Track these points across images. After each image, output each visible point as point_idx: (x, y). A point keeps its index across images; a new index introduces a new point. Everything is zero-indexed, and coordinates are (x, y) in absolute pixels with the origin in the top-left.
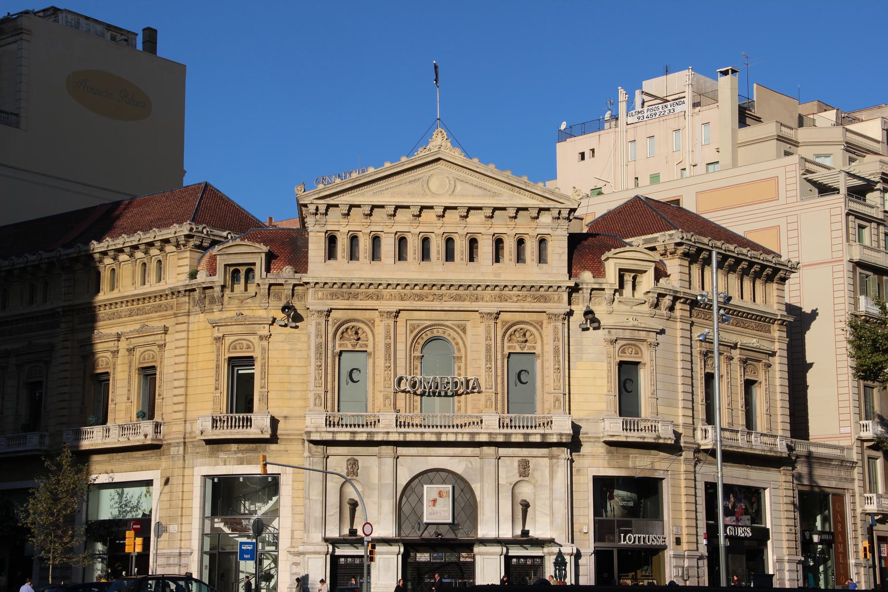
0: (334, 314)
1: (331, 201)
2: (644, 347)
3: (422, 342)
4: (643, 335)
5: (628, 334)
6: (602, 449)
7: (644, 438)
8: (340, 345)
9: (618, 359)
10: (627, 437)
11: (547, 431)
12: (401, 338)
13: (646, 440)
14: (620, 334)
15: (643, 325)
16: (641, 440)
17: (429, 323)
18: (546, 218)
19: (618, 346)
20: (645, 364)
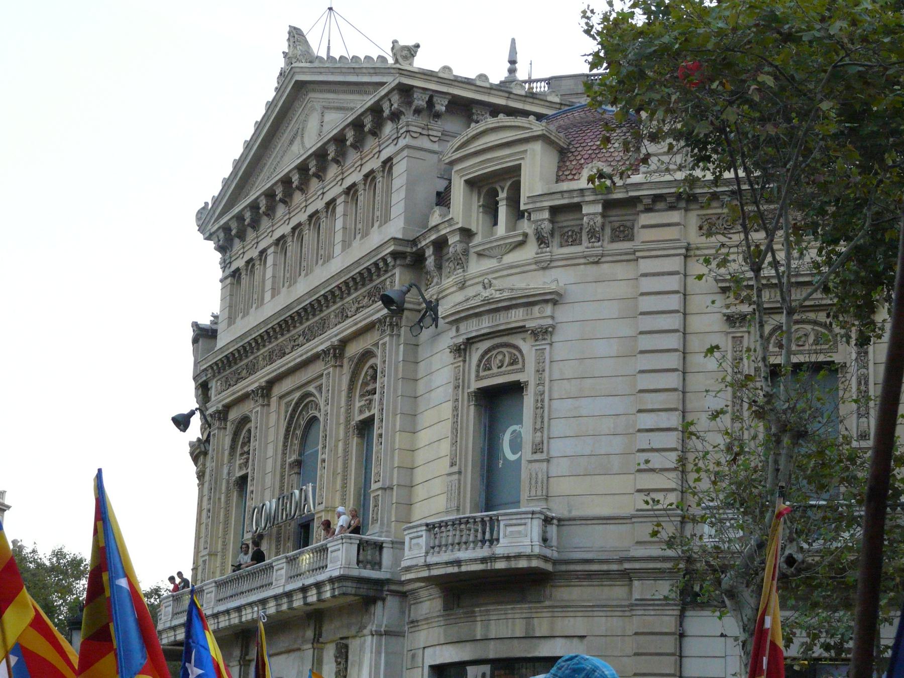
0: (234, 415)
1: (223, 221)
2: (526, 346)
3: (299, 432)
4: (516, 317)
5: (485, 325)
6: (430, 604)
7: (458, 563)
8: (240, 468)
9: (475, 385)
10: (428, 566)
11: (322, 577)
12: (271, 438)
13: (464, 569)
14: (472, 328)
15: (506, 294)
16: (455, 570)
17: (297, 395)
18: (388, 129)
19: (475, 357)
20: (526, 383)
